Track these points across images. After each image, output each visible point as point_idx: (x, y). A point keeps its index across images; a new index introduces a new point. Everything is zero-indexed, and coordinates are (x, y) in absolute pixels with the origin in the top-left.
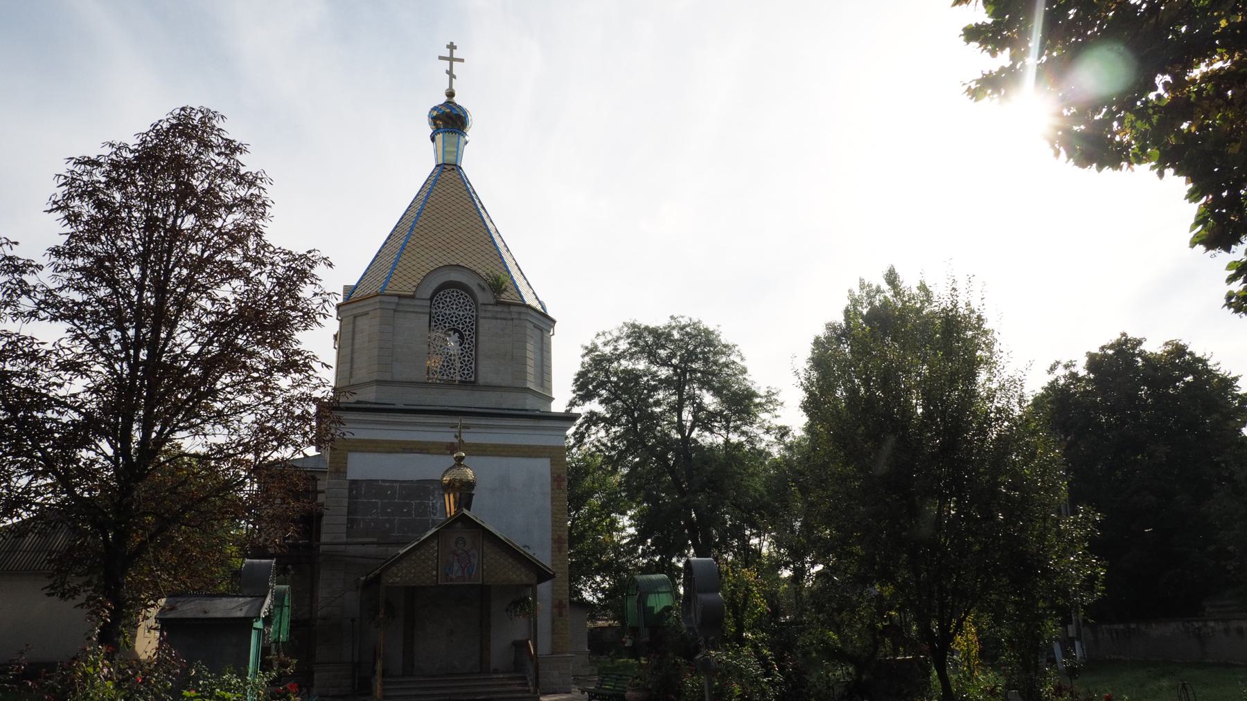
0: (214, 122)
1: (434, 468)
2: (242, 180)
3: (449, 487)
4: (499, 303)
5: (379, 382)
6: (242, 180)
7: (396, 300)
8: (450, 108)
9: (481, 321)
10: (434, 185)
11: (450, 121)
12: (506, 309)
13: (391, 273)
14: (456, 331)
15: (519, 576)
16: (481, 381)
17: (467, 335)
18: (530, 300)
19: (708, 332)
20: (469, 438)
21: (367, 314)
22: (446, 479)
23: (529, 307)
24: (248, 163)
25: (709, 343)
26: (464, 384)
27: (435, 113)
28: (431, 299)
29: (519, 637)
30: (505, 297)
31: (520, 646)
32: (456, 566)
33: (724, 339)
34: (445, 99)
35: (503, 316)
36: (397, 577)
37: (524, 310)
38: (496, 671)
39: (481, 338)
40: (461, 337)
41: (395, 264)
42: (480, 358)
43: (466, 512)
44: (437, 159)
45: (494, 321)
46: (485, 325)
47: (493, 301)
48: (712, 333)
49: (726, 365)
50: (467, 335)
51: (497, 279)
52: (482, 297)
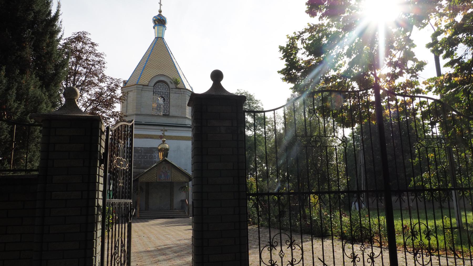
0: (87, 36)
1: (155, 143)
2: (97, 55)
3: (160, 150)
4: (177, 88)
5: (137, 115)
6: (97, 55)
7: (142, 86)
8: (160, 17)
9: (171, 94)
10: (154, 45)
11: (160, 21)
12: (179, 90)
13: (140, 77)
14: (162, 97)
15: (183, 179)
16: (171, 115)
17: (166, 98)
18: (188, 87)
19: (250, 95)
20: (167, 134)
21: (132, 91)
22: (159, 148)
23: (187, 89)
24: (98, 50)
25: (251, 99)
26: (164, 115)
27: (155, 19)
28: (154, 86)
29: (183, 198)
30: (179, 86)
31: (183, 201)
32: (163, 176)
33: (256, 98)
34: (158, 13)
35: (178, 92)
36: (143, 179)
37: (185, 90)
38: (175, 209)
39: (171, 100)
40: (164, 99)
41: (141, 73)
42: (170, 107)
43: (166, 158)
44: (155, 35)
46: (172, 95)
47: (175, 87)
48: (252, 96)
49: (257, 107)
50: (166, 98)
51: (176, 80)
52: (172, 86)
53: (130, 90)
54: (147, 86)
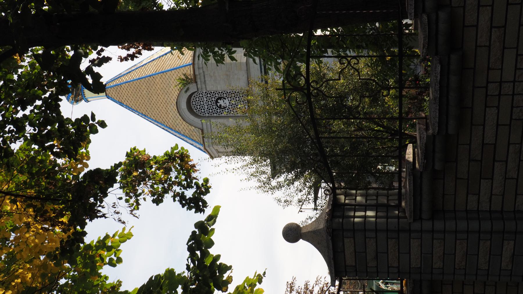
14: (217, 102)
35: (202, 78)
40: (220, 98)
45: (207, 82)
53: (215, 152)
54: (202, 130)
